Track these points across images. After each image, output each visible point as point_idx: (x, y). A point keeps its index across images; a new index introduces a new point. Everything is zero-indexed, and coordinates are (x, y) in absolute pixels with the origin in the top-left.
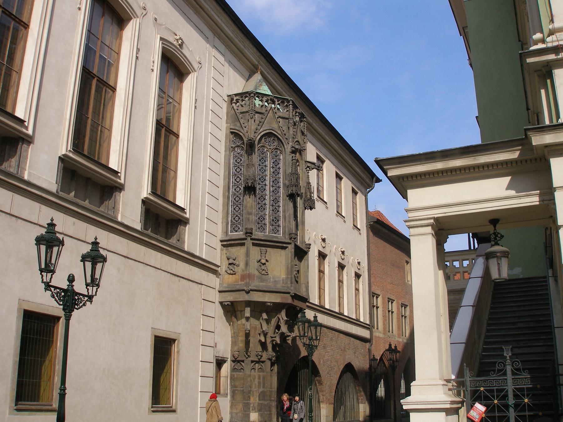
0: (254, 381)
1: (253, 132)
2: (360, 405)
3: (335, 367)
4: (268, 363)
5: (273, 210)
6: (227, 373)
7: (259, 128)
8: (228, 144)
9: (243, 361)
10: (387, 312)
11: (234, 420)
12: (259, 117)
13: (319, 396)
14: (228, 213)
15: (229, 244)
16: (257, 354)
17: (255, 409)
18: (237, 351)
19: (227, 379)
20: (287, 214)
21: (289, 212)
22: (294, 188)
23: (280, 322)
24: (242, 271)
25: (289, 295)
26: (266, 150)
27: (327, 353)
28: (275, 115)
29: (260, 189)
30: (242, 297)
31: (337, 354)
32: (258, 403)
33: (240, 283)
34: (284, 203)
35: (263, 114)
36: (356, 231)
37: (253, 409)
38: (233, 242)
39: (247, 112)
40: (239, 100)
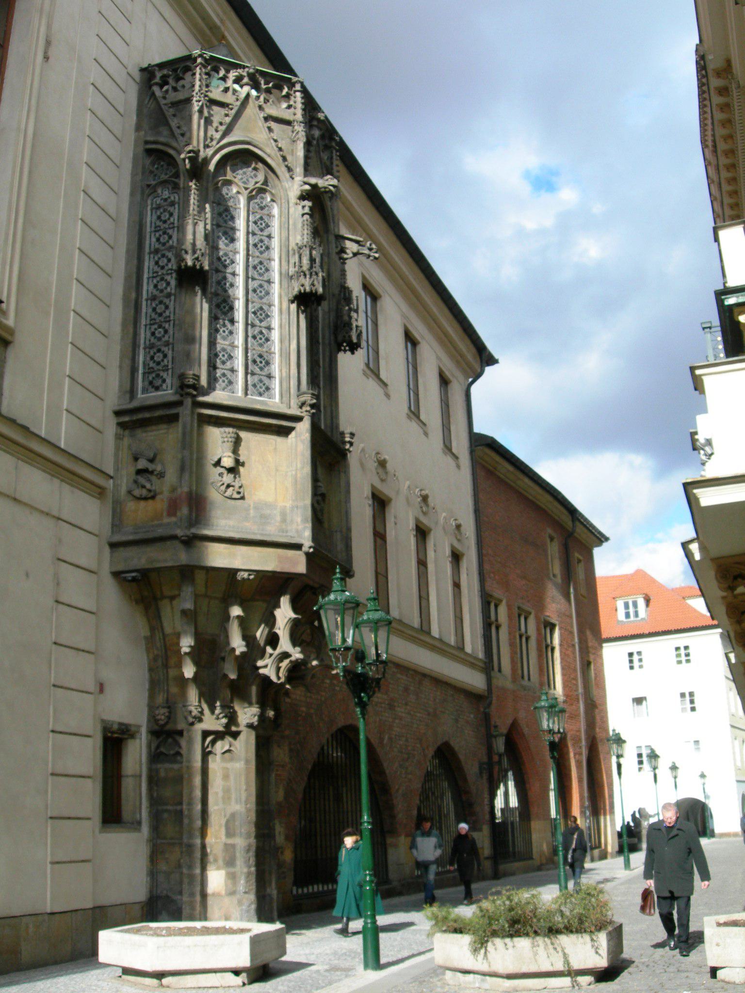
8: (139, 177)
10: (518, 637)
14: (135, 345)
15: (138, 420)
18: (164, 707)
32: (226, 844)
33: (166, 520)
36: (449, 459)
38: (147, 415)
40: (167, 76)
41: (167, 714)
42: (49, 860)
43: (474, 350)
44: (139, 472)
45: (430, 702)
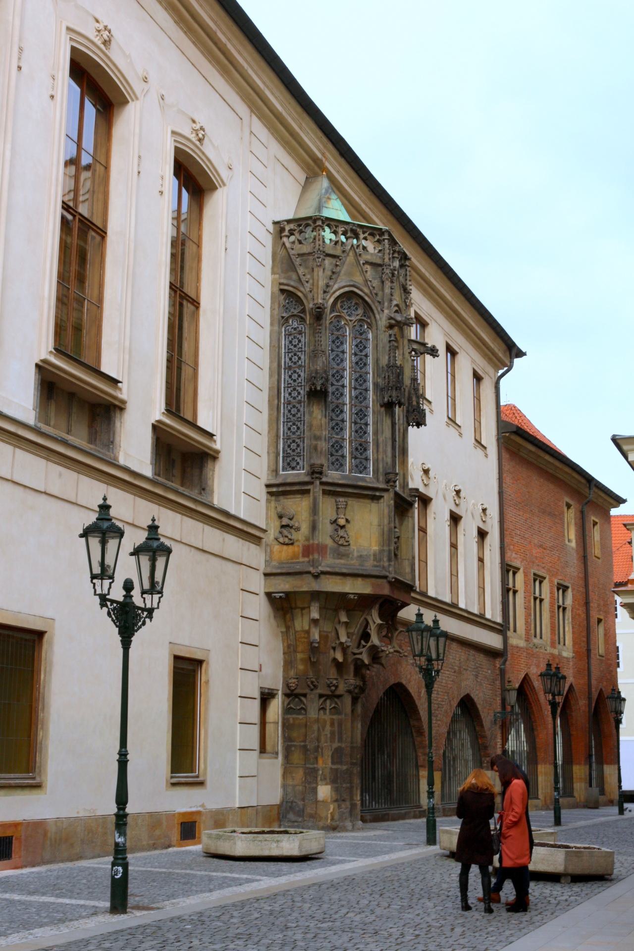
0: (323, 730)
1: (322, 292)
3: (444, 703)
4: (348, 700)
5: (356, 432)
6: (277, 716)
7: (332, 284)
8: (276, 312)
9: (305, 695)
12: (331, 264)
13: (417, 756)
14: (278, 436)
15: (281, 491)
17: (325, 779)
18: (294, 678)
20: (381, 439)
21: (384, 435)
22: (394, 394)
23: (369, 628)
25: (385, 581)
26: (343, 323)
28: (359, 258)
30: (307, 585)
31: (447, 679)
32: (331, 769)
33: (301, 560)
34: (376, 419)
36: (479, 451)
37: (323, 778)
38: (288, 488)
39: (309, 254)
40: (295, 230)
43: (504, 346)
44: (283, 527)
45: (457, 662)
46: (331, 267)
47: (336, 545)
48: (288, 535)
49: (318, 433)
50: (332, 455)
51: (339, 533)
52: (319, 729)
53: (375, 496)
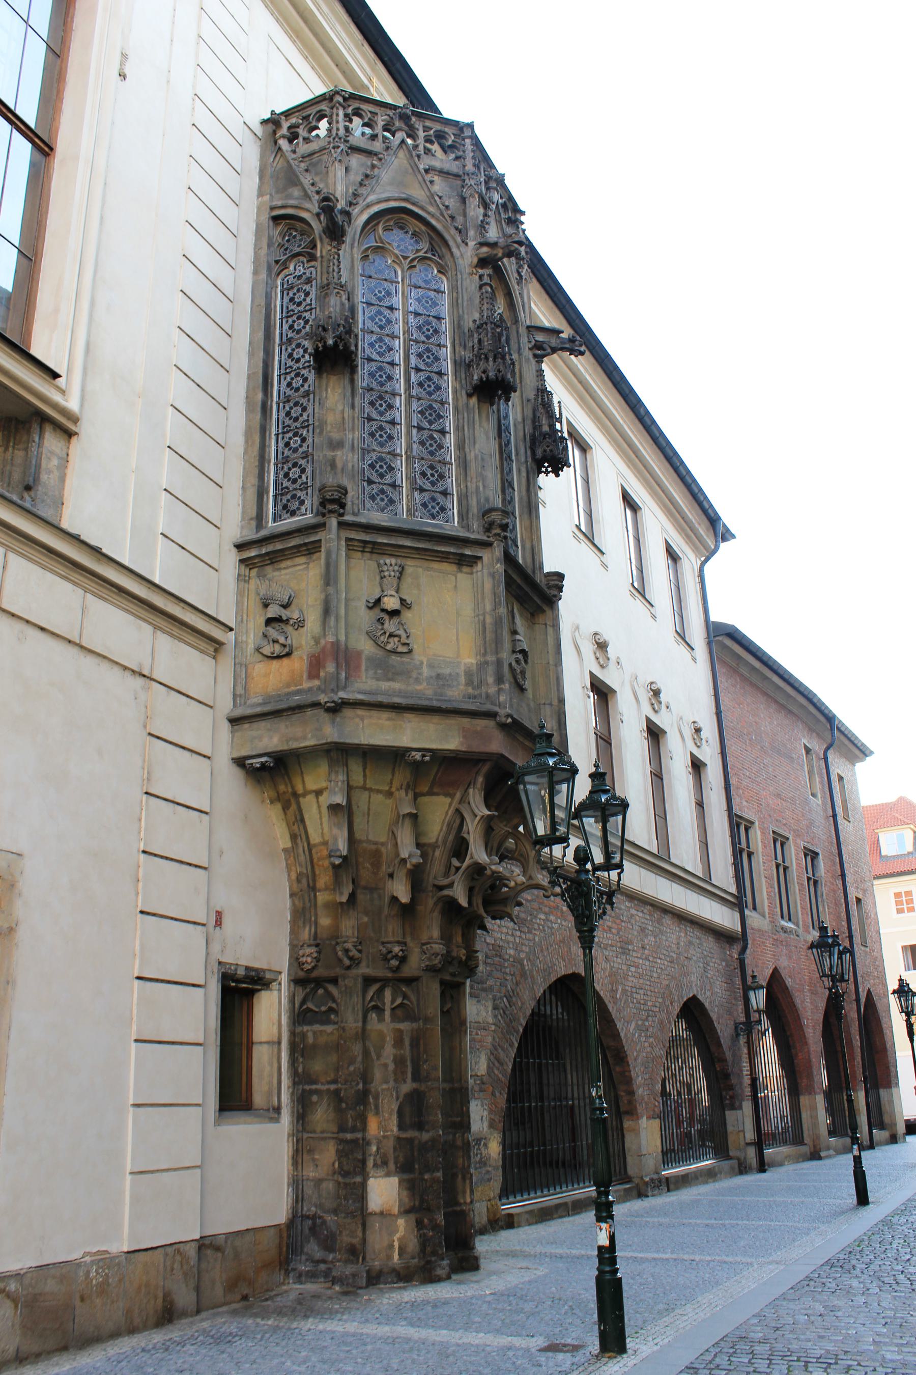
0: (379, 1056)
2: (727, 1113)
4: (433, 990)
5: (422, 443)
6: (275, 1030)
8: (264, 250)
9: (334, 981)
11: (309, 1210)
15: (267, 554)
16: (384, 950)
17: (385, 1163)
18: (309, 946)
19: (276, 1050)
21: (477, 446)
23: (465, 828)
24: (313, 643)
27: (633, 969)
29: (372, 375)
31: (659, 971)
32: (398, 1139)
33: (306, 685)
35: (376, 154)
36: (682, 649)
37: (379, 1162)
38: (279, 546)
41: (315, 955)
42: (129, 1169)
44: (269, 622)
46: (363, 170)
47: (380, 653)
48: (279, 638)
49: (336, 436)
50: (370, 482)
51: (386, 626)
52: (366, 1053)
53: (463, 555)
